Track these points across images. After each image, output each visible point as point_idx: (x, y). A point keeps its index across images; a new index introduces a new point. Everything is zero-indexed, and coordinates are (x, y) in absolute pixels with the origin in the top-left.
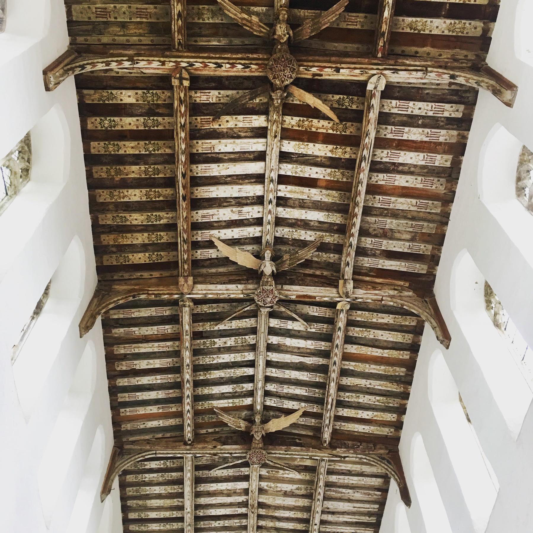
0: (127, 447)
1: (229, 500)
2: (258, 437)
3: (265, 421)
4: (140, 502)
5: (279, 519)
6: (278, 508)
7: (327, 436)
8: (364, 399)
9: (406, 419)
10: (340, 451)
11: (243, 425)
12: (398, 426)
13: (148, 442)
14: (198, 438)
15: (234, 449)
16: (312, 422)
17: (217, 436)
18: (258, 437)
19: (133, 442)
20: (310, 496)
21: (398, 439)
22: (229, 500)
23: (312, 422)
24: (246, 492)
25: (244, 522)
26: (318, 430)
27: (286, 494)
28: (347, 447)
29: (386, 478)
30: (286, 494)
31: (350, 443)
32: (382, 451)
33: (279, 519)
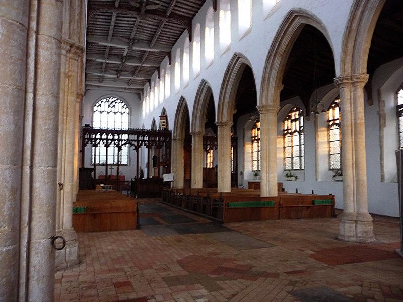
0: (93, 6)
1: (128, 23)
2: (143, 11)
3: (147, 4)
4: (94, 19)
5: (145, 30)
6: (145, 27)
7: (168, 14)
8: (183, 6)
9: (197, 14)
10: (171, 19)
11: (138, 5)
12: (194, 15)
13: (101, 5)
14: (120, 7)
15: (134, 14)
16: (164, 8)
17: (127, 6)
18: (143, 11)
19: (95, 4)
20: (158, 26)
21: (193, 18)
22: (128, 23)
23: (164, 8)
24: (135, 21)
25: (132, 28)
26: (165, 12)
27: (149, 24)
28: (175, 18)
29: (184, 29)
30: (149, 24)
31: (176, 16)
32: (187, 21)
33: (145, 30)
